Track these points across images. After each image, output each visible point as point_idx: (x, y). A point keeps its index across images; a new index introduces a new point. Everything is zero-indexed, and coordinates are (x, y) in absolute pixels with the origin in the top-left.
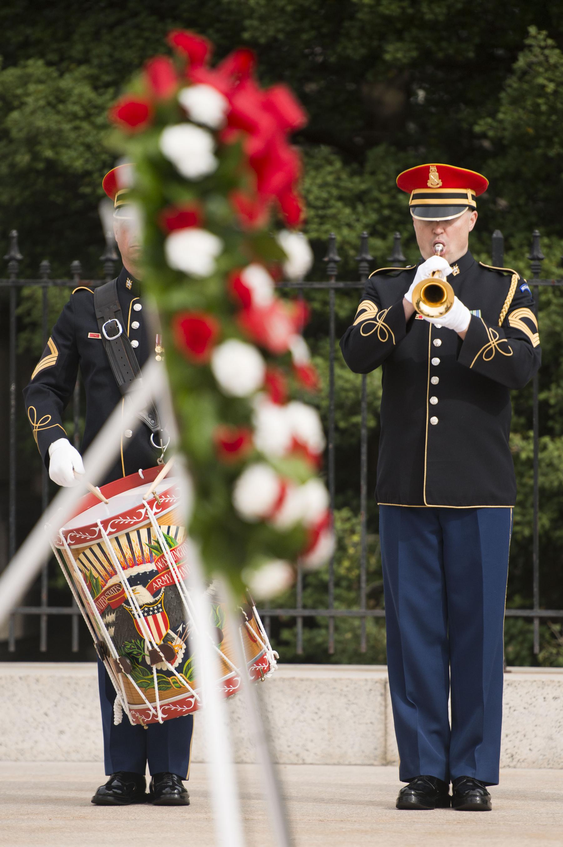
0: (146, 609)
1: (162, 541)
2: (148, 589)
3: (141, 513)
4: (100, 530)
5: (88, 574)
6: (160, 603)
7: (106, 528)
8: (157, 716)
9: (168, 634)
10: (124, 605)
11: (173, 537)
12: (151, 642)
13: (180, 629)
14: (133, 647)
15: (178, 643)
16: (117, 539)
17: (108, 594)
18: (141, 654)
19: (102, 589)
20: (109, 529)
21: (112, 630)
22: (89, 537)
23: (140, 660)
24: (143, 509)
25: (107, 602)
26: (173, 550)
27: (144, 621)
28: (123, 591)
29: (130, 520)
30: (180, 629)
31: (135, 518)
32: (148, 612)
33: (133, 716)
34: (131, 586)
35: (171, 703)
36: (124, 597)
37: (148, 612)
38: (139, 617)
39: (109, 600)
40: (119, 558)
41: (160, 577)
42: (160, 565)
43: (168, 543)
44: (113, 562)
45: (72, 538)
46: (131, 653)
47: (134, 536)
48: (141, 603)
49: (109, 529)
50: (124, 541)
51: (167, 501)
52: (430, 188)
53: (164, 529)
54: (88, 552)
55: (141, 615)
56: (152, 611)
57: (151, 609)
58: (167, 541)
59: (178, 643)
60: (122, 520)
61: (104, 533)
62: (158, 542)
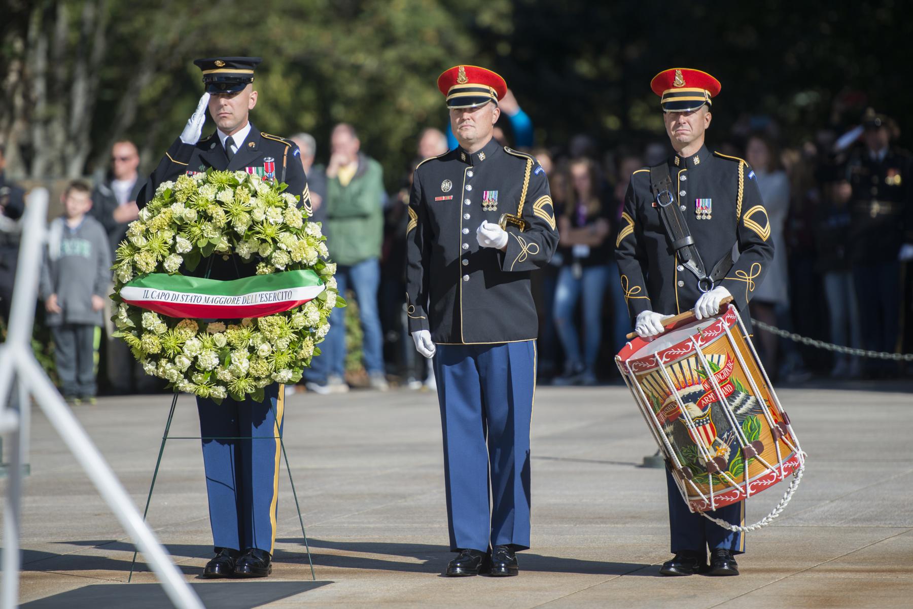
0: (697, 421)
1: (707, 366)
2: (698, 405)
3: (689, 346)
5: (650, 394)
6: (708, 416)
8: (711, 505)
9: (715, 440)
10: (680, 418)
11: (716, 363)
12: (702, 447)
13: (725, 436)
14: (688, 451)
15: (724, 447)
16: (671, 366)
17: (667, 410)
19: (662, 406)
20: (664, 359)
22: (649, 366)
23: (695, 461)
24: (690, 342)
26: (717, 373)
27: (696, 430)
28: (679, 408)
29: (680, 351)
30: (725, 436)
31: (684, 349)
32: (699, 423)
33: (692, 505)
34: (684, 403)
35: (721, 495)
36: (679, 412)
37: (699, 423)
38: (692, 427)
39: (668, 414)
40: (674, 380)
41: (707, 396)
43: (712, 368)
45: (636, 367)
46: (687, 456)
47: (684, 363)
48: (693, 417)
49: (664, 359)
51: (709, 335)
52: (676, 87)
53: (709, 357)
54: (649, 377)
55: (694, 426)
56: (702, 422)
57: (701, 421)
58: (711, 366)
59: (724, 447)
60: (674, 352)
61: (661, 362)
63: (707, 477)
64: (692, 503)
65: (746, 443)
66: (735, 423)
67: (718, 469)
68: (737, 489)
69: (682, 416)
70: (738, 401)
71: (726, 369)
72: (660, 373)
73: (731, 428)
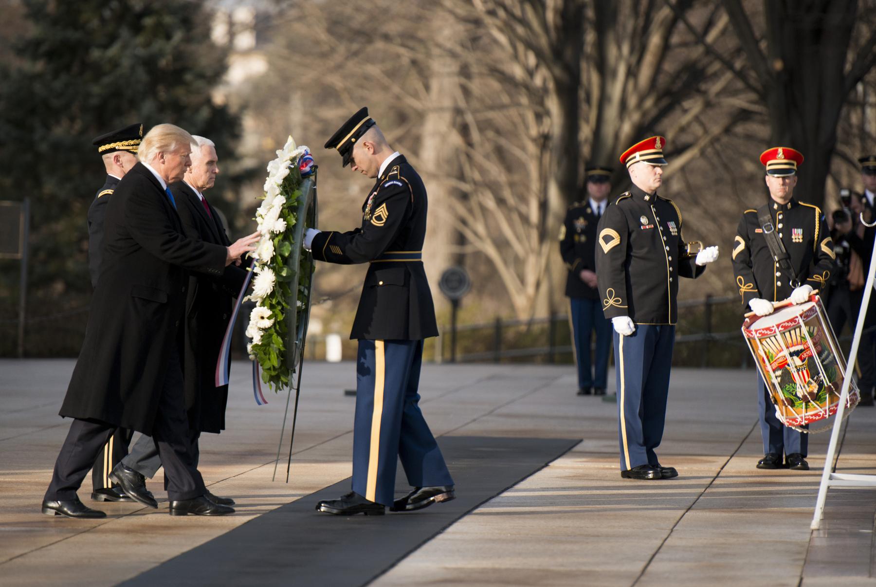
4: (775, 330)
5: (767, 351)
7: (778, 328)
9: (809, 381)
10: (786, 366)
13: (815, 378)
18: (794, 391)
20: (780, 329)
21: (779, 379)
23: (794, 394)
25: (777, 365)
28: (786, 359)
30: (815, 378)
39: (779, 364)
42: (806, 347)
44: (781, 345)
47: (793, 332)
49: (780, 329)
50: (787, 334)
54: (768, 340)
55: (796, 372)
60: (787, 324)
61: (777, 331)
62: (804, 335)
63: (802, 403)
64: (788, 420)
65: (827, 383)
66: (821, 370)
67: (810, 399)
68: (821, 412)
69: (789, 365)
70: (824, 356)
71: (817, 336)
72: (776, 337)
73: (819, 373)
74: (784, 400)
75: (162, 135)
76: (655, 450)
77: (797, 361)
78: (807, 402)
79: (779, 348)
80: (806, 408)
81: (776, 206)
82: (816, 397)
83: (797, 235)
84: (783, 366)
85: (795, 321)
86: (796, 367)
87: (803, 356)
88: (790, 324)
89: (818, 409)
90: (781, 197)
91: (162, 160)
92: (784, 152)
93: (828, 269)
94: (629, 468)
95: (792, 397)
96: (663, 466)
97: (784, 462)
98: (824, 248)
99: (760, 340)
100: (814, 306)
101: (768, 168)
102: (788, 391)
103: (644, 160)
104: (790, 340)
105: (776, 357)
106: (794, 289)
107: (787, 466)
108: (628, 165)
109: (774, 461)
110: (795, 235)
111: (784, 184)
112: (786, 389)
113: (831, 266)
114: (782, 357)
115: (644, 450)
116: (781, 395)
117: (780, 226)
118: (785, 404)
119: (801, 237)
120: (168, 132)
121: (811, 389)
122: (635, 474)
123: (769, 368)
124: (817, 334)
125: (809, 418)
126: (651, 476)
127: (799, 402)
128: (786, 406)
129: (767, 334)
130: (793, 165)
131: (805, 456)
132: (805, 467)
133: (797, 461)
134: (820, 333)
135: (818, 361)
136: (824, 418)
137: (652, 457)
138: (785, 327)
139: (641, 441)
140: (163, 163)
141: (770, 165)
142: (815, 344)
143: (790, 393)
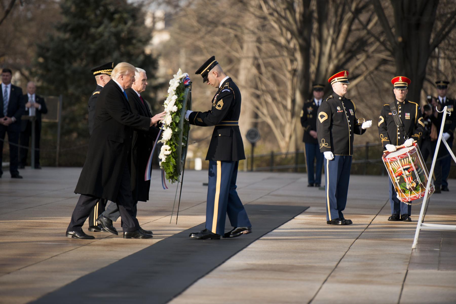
5: (393, 168)
7: (398, 158)
9: (412, 182)
10: (402, 175)
13: (415, 180)
20: (399, 158)
21: (399, 180)
23: (405, 187)
25: (398, 174)
28: (402, 172)
30: (415, 180)
42: (411, 166)
44: (400, 165)
47: (405, 159)
49: (399, 158)
50: (403, 160)
54: (394, 163)
60: (402, 156)
61: (398, 159)
62: (410, 161)
63: (409, 192)
64: (402, 199)
65: (420, 182)
67: (412, 190)
69: (403, 174)
70: (419, 170)
72: (397, 161)
74: (401, 190)
75: (122, 67)
76: (342, 212)
77: (407, 173)
78: (411, 191)
79: (399, 167)
80: (411, 194)
81: (398, 103)
82: (415, 189)
83: (408, 116)
84: (400, 175)
85: (406, 155)
86: (406, 175)
87: (409, 170)
88: (404, 156)
89: (416, 194)
90: (401, 99)
91: (122, 79)
92: (402, 78)
93: (421, 131)
94: (330, 220)
95: (404, 189)
96: (346, 219)
97: (400, 218)
98: (420, 122)
99: (390, 163)
100: (415, 148)
101: (395, 86)
102: (402, 186)
103: (339, 81)
104: (404, 163)
105: (397, 171)
106: (406, 140)
107: (401, 220)
108: (332, 83)
109: (396, 218)
110: (407, 116)
111: (402, 93)
112: (402, 185)
113: (422, 130)
114: (400, 170)
115: (337, 212)
116: (399, 188)
117: (400, 112)
118: (401, 192)
119: (409, 117)
120: (125, 66)
121: (413, 185)
122: (333, 222)
123: (394, 176)
124: (416, 161)
125: (412, 198)
126: (340, 223)
127: (408, 191)
128: (402, 193)
129: (393, 160)
130: (406, 84)
131: (410, 216)
132: (410, 220)
133: (406, 217)
134: (417, 160)
135: (416, 173)
136: (418, 198)
137: (341, 215)
138: (402, 157)
139: (336, 208)
140: (123, 80)
141: (396, 84)
142: (415, 165)
143: (403, 187)
